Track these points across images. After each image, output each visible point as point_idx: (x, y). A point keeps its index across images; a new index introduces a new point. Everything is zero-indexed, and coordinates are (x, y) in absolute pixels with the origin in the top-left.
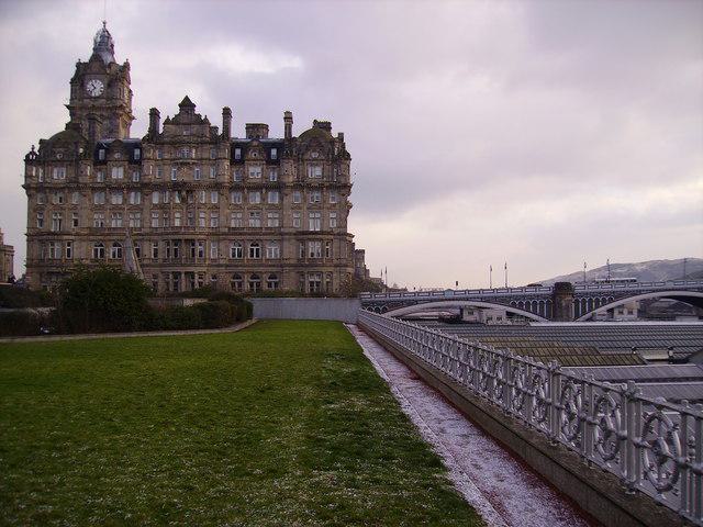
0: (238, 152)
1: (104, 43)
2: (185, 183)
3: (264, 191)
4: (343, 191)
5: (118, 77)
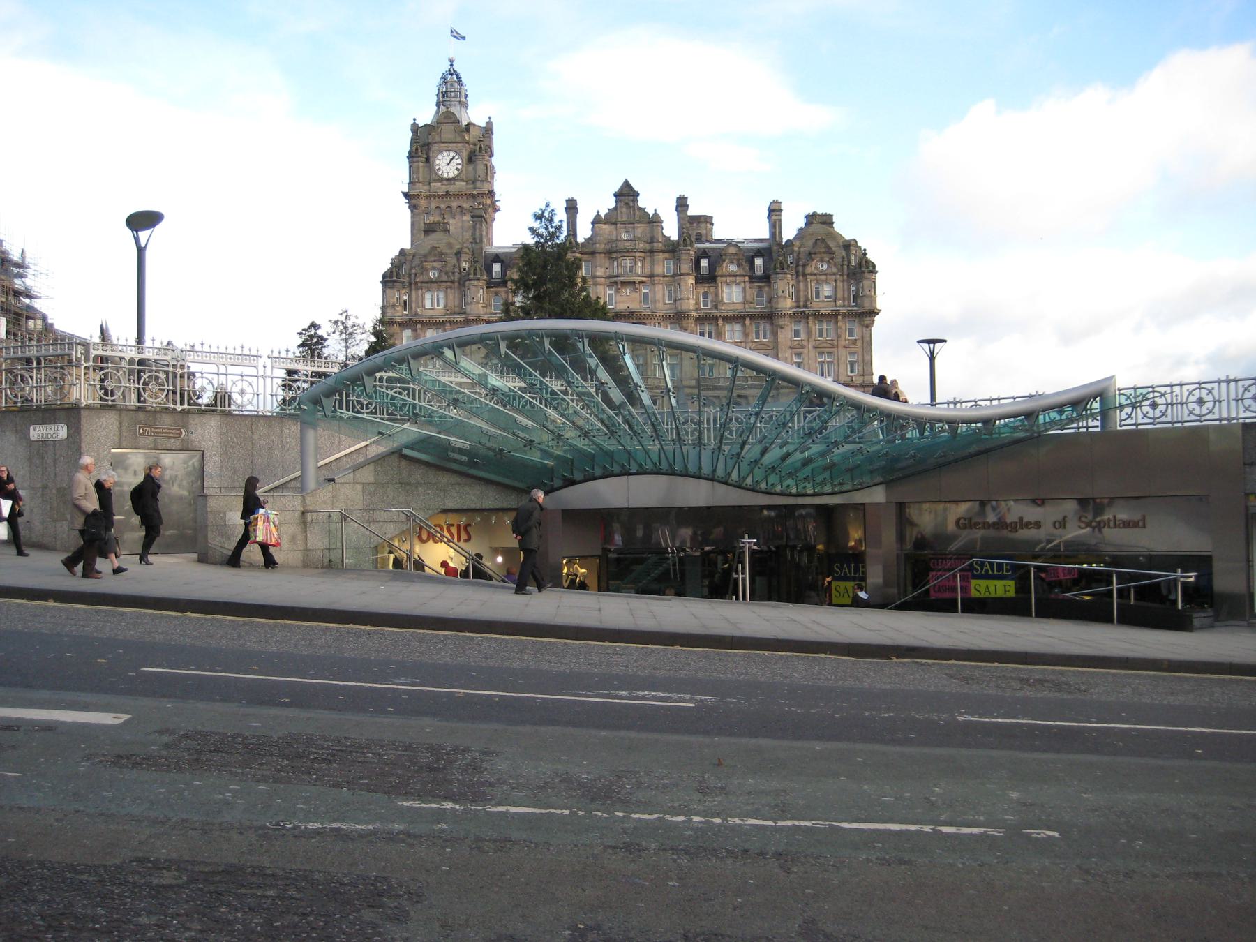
0: (704, 263)
1: (451, 90)
2: (632, 313)
3: (748, 322)
4: (867, 320)
5: (478, 147)
